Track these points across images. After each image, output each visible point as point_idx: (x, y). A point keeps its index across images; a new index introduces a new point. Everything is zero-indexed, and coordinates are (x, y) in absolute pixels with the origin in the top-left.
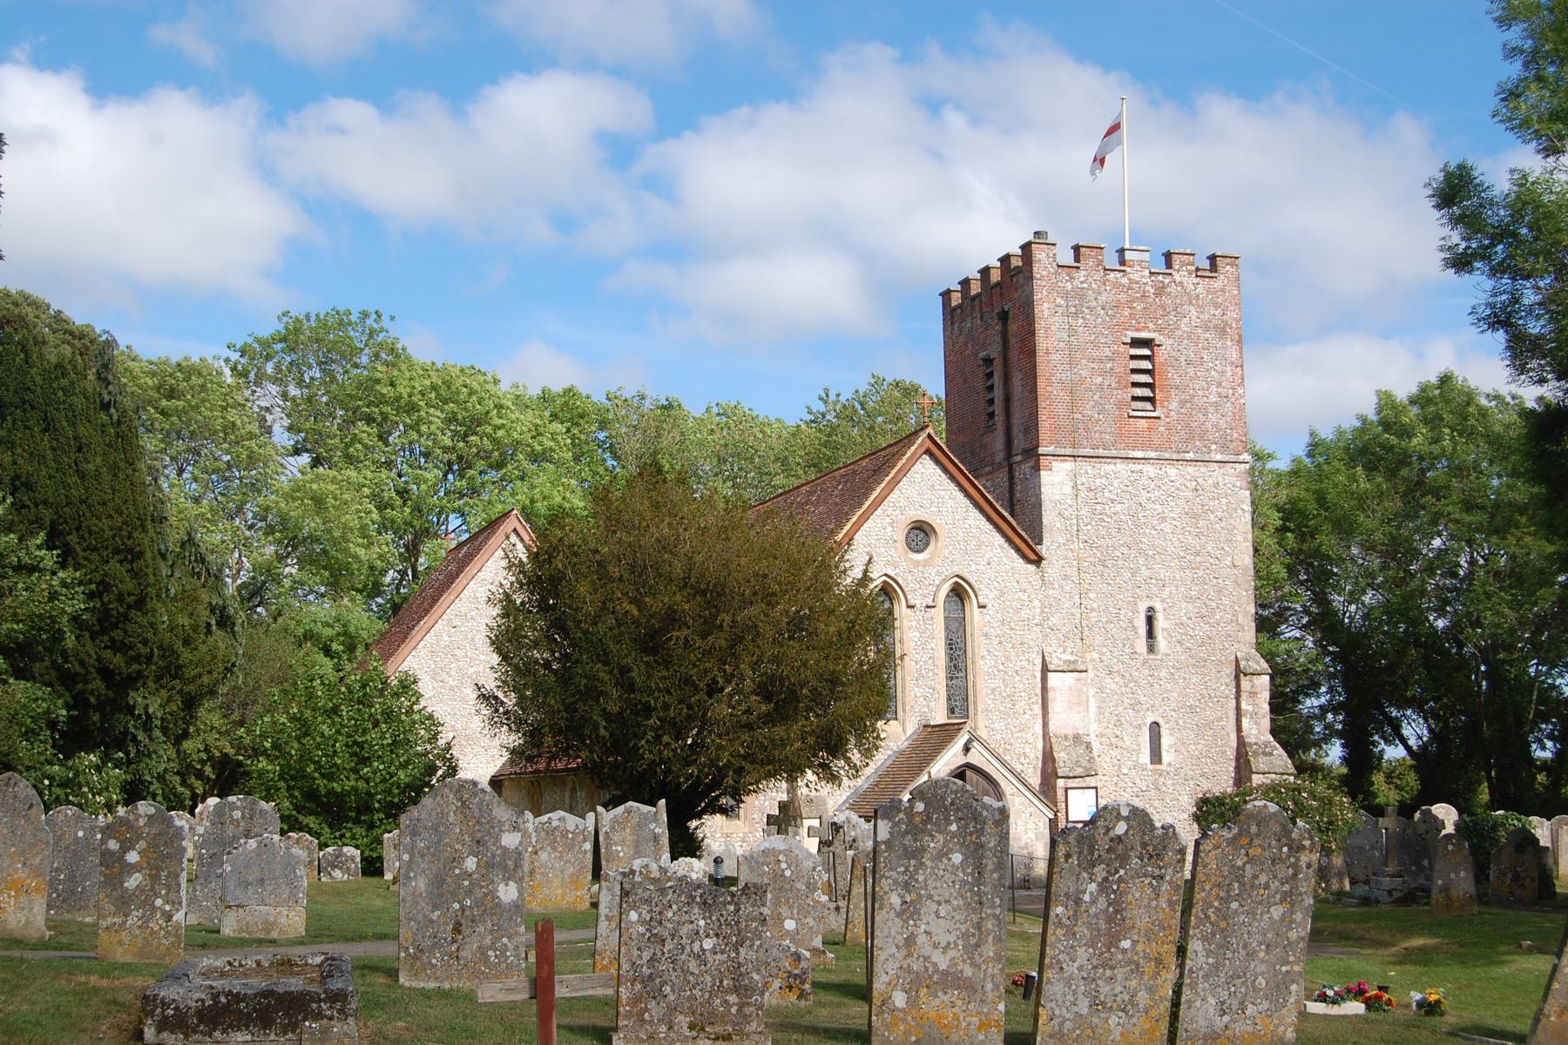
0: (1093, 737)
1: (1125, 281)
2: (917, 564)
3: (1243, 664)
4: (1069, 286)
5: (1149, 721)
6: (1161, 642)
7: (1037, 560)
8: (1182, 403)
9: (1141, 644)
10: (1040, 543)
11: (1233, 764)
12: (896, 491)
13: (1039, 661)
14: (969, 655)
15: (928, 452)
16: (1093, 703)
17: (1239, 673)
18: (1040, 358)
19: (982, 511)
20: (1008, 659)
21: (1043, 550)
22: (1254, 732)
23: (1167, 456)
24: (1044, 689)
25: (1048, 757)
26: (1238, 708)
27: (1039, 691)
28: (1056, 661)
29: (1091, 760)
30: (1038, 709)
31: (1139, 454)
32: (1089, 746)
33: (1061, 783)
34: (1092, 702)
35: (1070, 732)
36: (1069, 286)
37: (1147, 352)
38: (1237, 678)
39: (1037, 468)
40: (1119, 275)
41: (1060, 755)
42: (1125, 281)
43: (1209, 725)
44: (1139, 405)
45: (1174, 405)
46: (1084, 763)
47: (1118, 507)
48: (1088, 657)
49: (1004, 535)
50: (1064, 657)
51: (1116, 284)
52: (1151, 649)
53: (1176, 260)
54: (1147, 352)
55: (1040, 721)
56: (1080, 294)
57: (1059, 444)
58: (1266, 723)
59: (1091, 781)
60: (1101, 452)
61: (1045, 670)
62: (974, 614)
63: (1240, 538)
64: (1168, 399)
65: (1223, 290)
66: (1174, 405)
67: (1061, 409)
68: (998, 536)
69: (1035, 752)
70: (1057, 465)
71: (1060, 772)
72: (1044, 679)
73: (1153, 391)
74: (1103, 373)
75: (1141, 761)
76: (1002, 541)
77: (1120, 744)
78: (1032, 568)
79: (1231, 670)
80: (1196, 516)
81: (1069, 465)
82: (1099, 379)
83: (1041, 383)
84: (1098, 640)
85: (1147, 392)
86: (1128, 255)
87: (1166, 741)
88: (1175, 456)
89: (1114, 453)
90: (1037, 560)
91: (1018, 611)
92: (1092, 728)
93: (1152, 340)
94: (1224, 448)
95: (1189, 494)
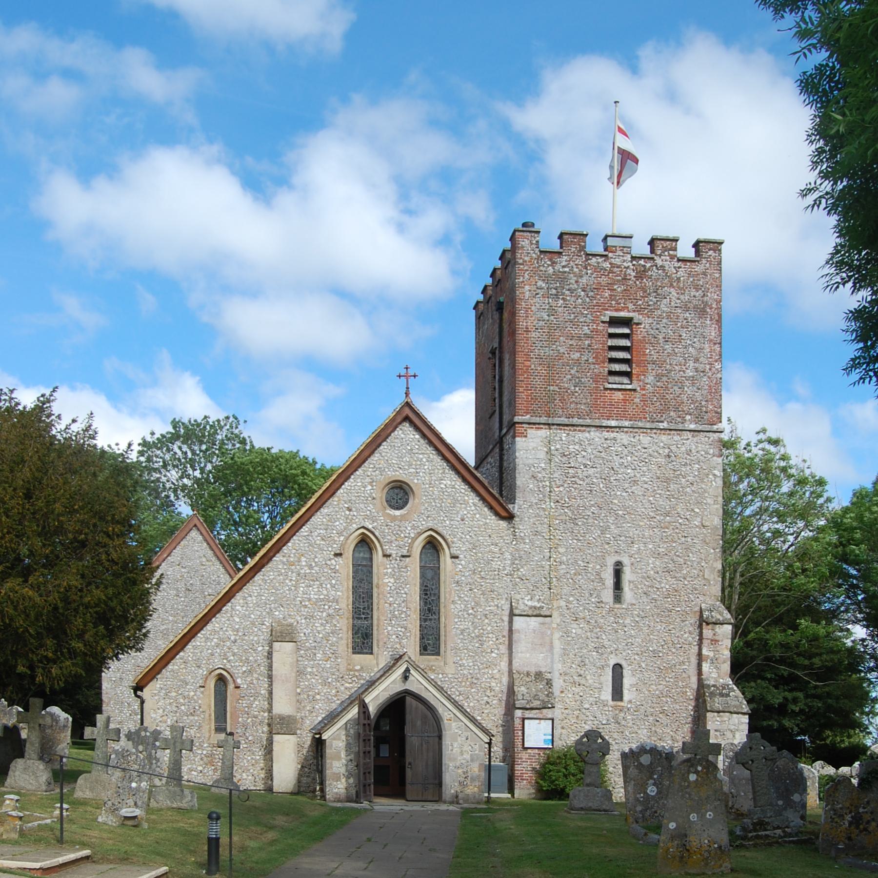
0: (556, 674)
1: (607, 265)
2: (394, 518)
3: (706, 614)
4: (551, 270)
5: (612, 662)
6: (628, 593)
7: (509, 517)
8: (659, 377)
9: (608, 595)
10: (512, 500)
11: (693, 703)
12: (377, 455)
13: (507, 607)
14: (442, 600)
15: (407, 419)
16: (558, 645)
17: (703, 622)
18: (520, 336)
19: (458, 472)
20: (477, 604)
21: (515, 509)
22: (714, 675)
23: (640, 424)
24: (511, 631)
25: (511, 691)
26: (700, 654)
27: (506, 633)
28: (522, 607)
29: (550, 694)
30: (504, 649)
31: (613, 423)
32: (549, 683)
33: (518, 713)
34: (558, 645)
35: (533, 670)
36: (551, 270)
37: (626, 331)
38: (700, 627)
39: (514, 437)
40: (600, 260)
41: (521, 690)
42: (607, 265)
43: (672, 668)
44: (617, 379)
45: (650, 379)
46: (542, 696)
47: (591, 471)
48: (555, 604)
49: (479, 494)
50: (530, 603)
51: (597, 269)
52: (618, 598)
53: (659, 246)
54: (626, 331)
55: (506, 659)
56: (561, 278)
57: (534, 413)
58: (726, 667)
59: (548, 713)
60: (575, 421)
61: (512, 615)
62: (446, 561)
63: (709, 501)
64: (644, 373)
65: (704, 274)
66: (650, 379)
67: (538, 382)
68: (472, 495)
69: (500, 686)
70: (532, 432)
71: (518, 704)
72: (511, 622)
73: (631, 367)
74: (581, 350)
75: (602, 698)
76: (476, 500)
77: (583, 682)
78: (503, 524)
79: (693, 619)
80: (668, 480)
81: (544, 432)
82: (577, 355)
83: (520, 359)
84: (566, 590)
85: (624, 368)
86: (610, 242)
87: (627, 682)
88: (648, 425)
89: (588, 421)
90: (509, 517)
91: (488, 562)
92: (556, 669)
93: (631, 319)
94: (698, 419)
95: (662, 460)
